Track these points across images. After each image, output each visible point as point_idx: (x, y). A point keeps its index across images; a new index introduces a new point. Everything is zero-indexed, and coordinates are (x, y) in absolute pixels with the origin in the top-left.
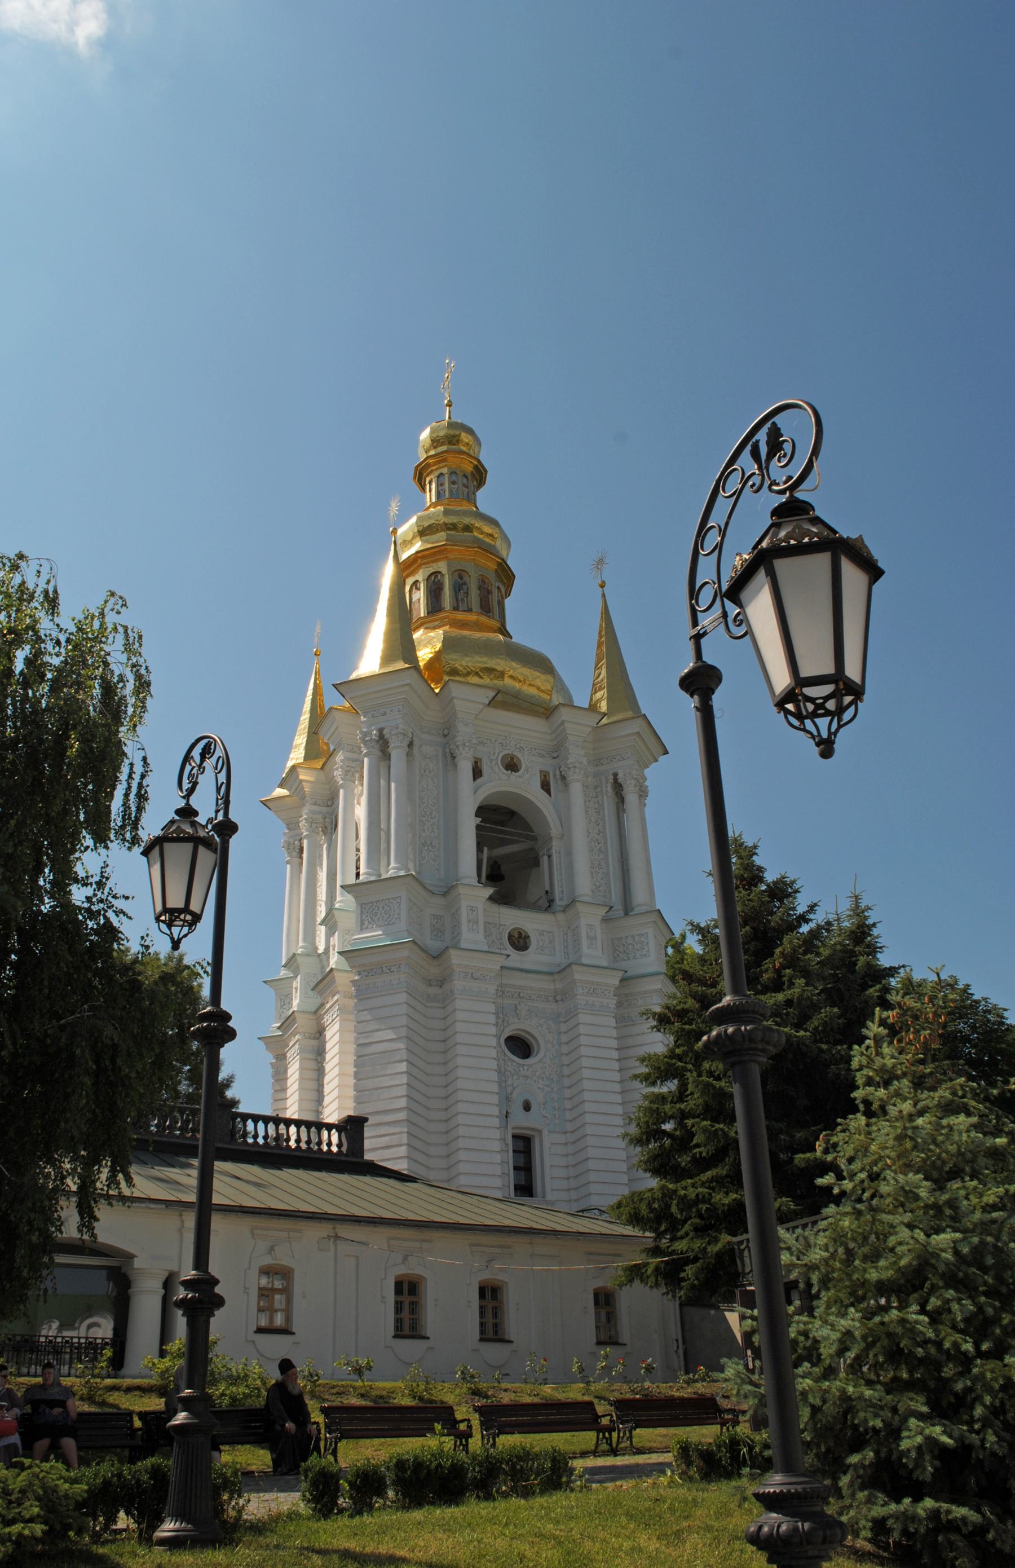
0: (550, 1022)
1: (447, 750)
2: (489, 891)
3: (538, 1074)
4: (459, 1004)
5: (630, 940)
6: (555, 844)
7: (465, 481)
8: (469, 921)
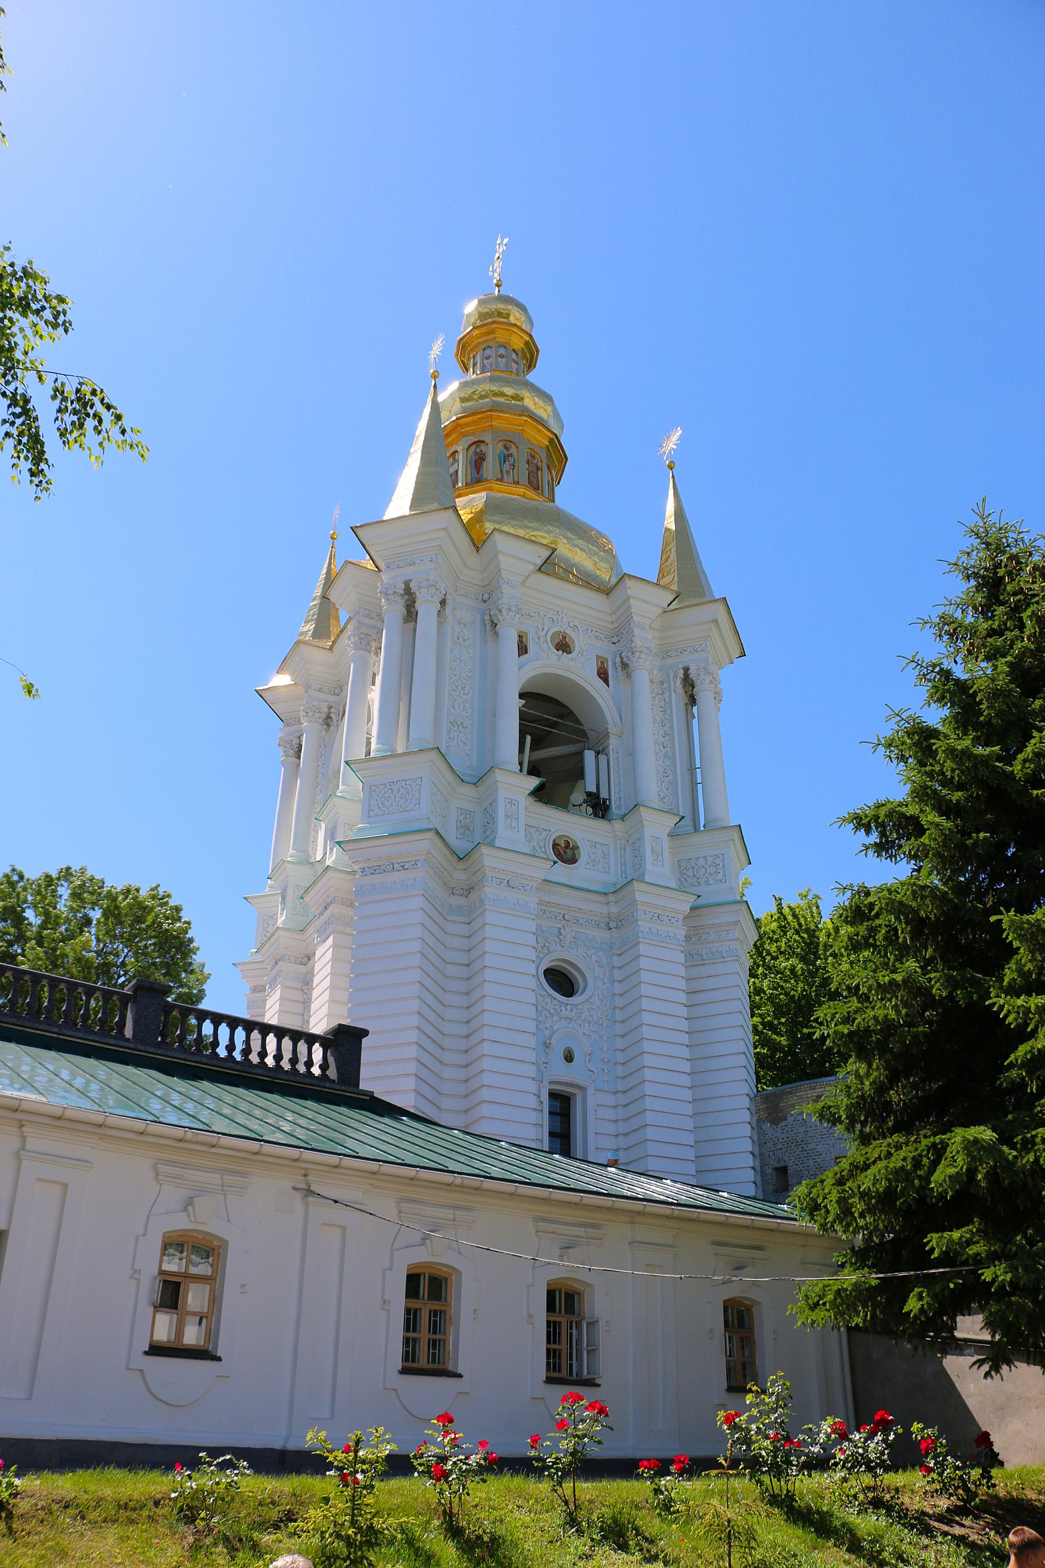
0: (601, 954)
1: (487, 617)
2: (534, 782)
4: (489, 917)
5: (701, 862)
6: (613, 743)
7: (514, 356)
8: (507, 816)
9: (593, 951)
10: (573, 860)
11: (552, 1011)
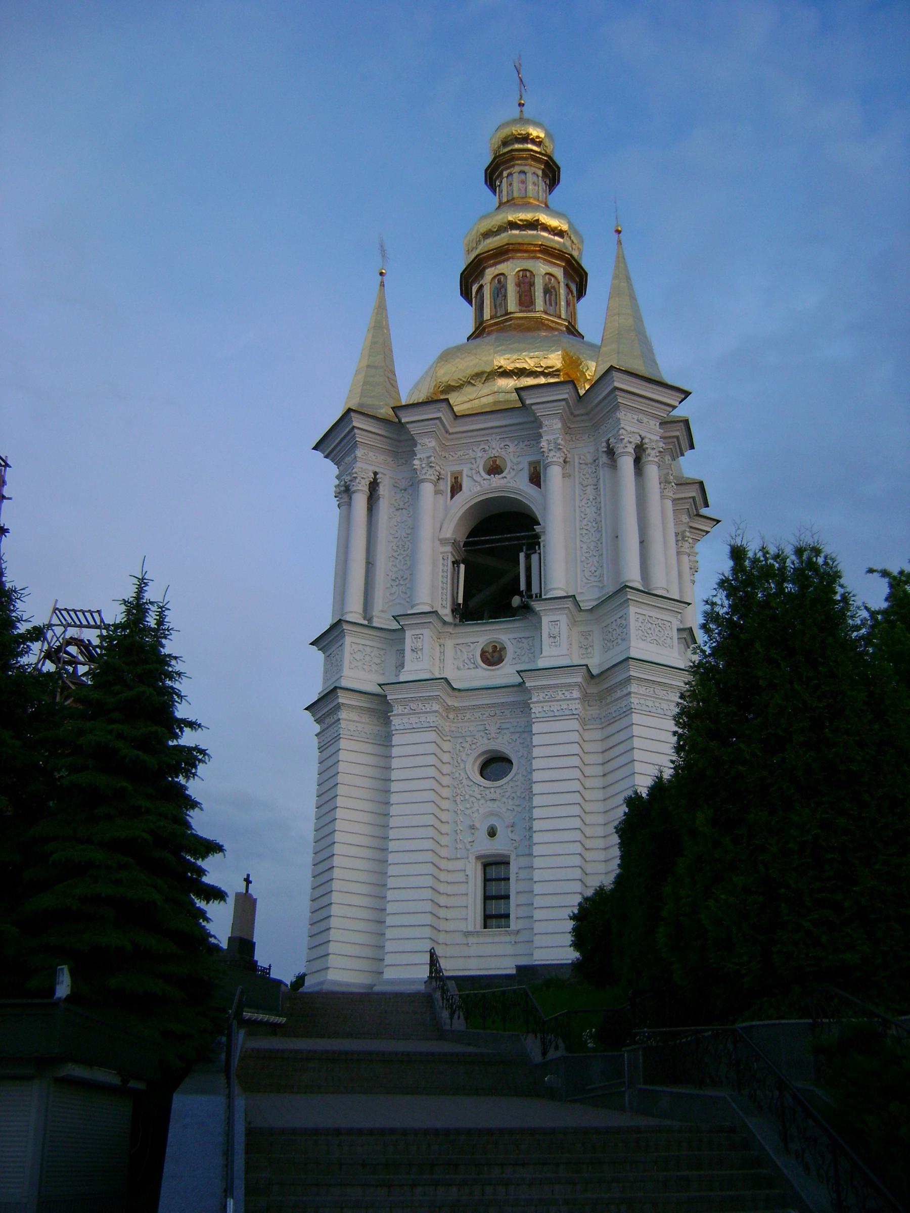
3: (507, 794)
9: (518, 735)
10: (500, 660)
11: (479, 797)
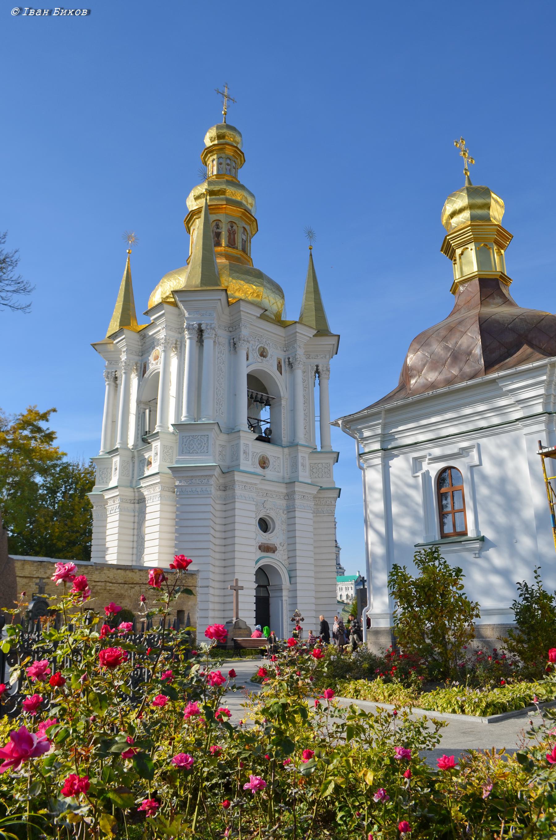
4: (237, 505)
